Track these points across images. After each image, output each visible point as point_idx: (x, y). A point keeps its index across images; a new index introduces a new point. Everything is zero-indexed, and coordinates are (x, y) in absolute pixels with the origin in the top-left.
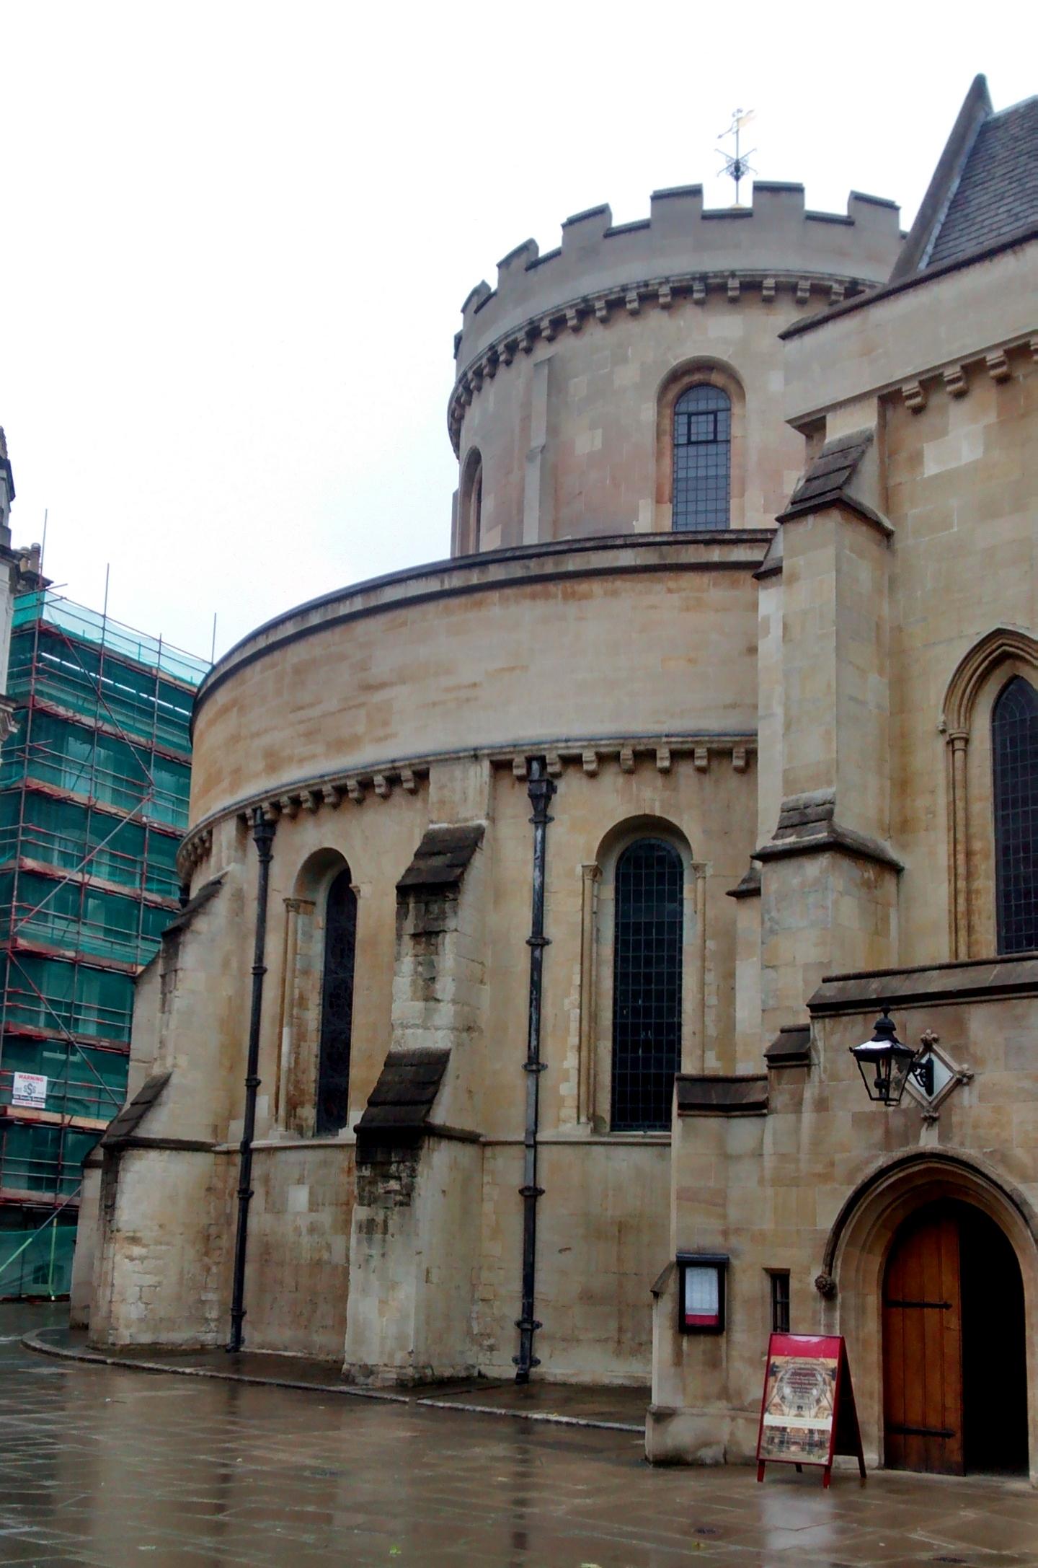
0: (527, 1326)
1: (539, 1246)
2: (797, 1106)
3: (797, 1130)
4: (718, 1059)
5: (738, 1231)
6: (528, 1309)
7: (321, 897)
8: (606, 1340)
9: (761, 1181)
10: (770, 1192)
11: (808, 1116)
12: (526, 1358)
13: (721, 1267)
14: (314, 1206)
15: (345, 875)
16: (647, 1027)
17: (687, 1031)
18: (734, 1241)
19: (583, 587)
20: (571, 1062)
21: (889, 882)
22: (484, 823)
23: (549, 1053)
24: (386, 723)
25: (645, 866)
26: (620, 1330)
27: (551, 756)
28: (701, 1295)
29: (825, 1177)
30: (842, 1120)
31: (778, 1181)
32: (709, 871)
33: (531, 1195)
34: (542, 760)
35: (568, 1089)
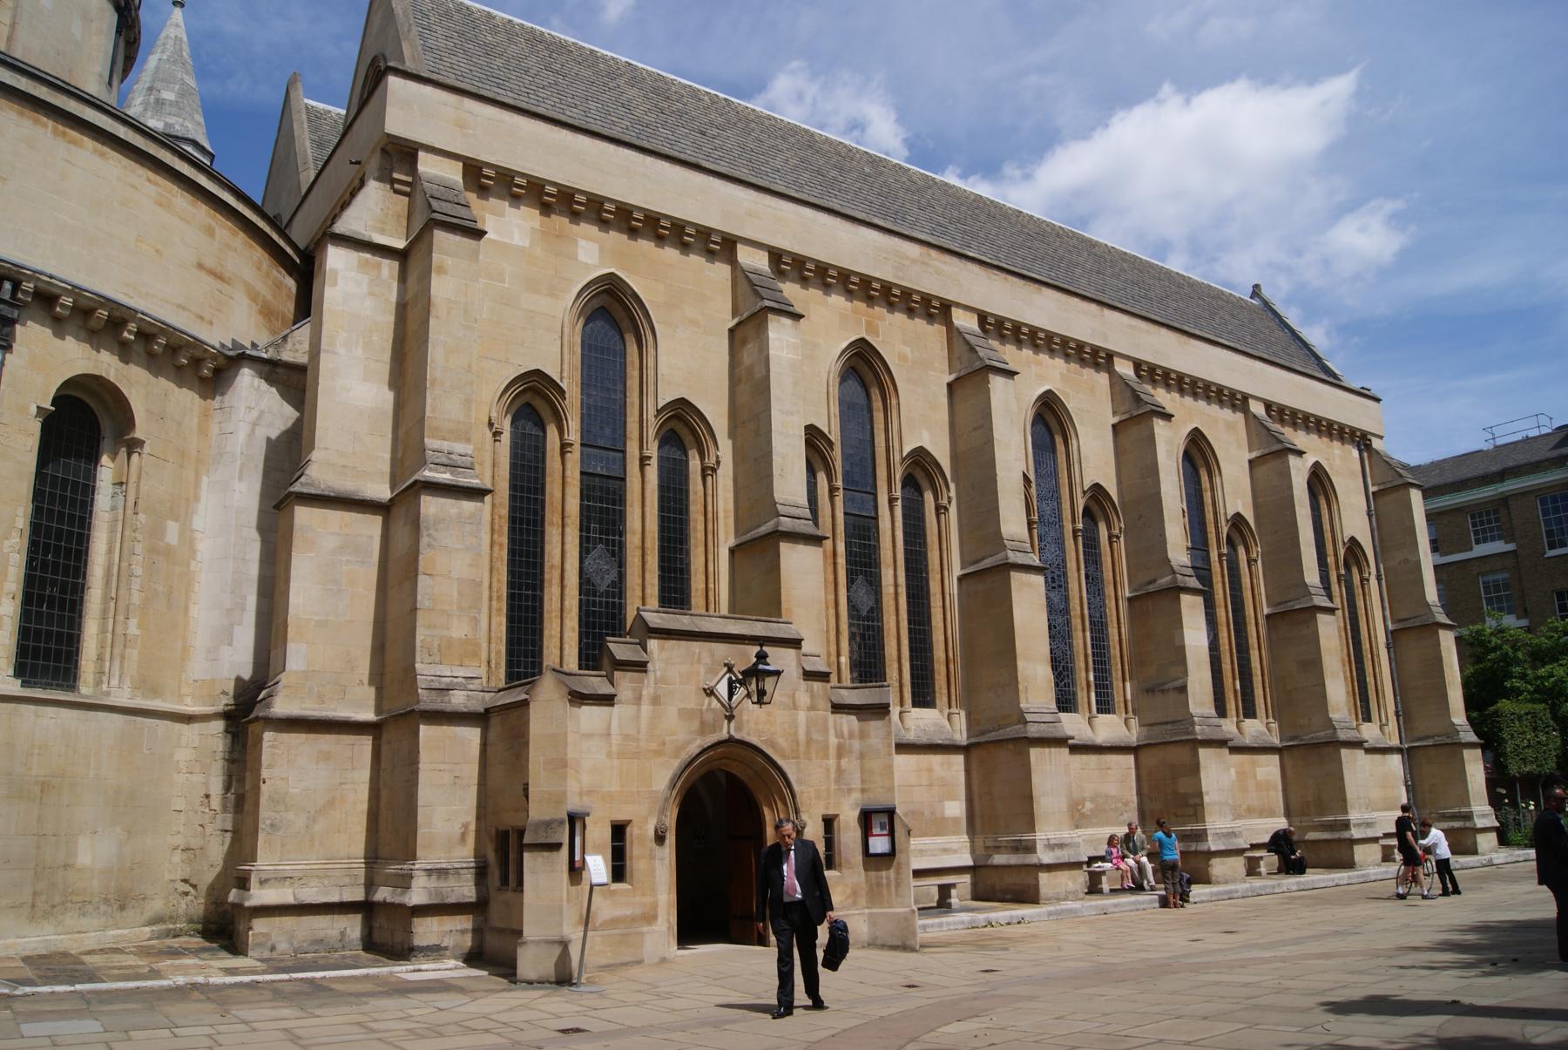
2: (638, 700)
3: (638, 717)
4: (139, 627)
5: (590, 792)
8: (21, 905)
9: (609, 755)
10: (616, 762)
11: (646, 708)
16: (54, 583)
18: (586, 800)
26: (35, 894)
27: (28, 286)
29: (658, 753)
30: (671, 712)
31: (620, 755)
32: (147, 449)
34: (16, 286)
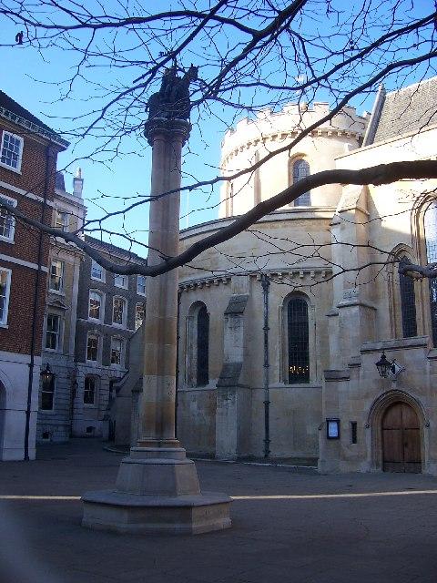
0: (267, 441)
1: (270, 419)
6: (267, 436)
7: (196, 315)
12: (267, 451)
13: (338, 421)
14: (199, 408)
15: (204, 308)
17: (311, 354)
19: (276, 224)
20: (277, 364)
21: (373, 312)
22: (248, 294)
23: (270, 363)
24: (216, 264)
25: (296, 304)
28: (333, 431)
33: (267, 404)
35: (277, 372)
